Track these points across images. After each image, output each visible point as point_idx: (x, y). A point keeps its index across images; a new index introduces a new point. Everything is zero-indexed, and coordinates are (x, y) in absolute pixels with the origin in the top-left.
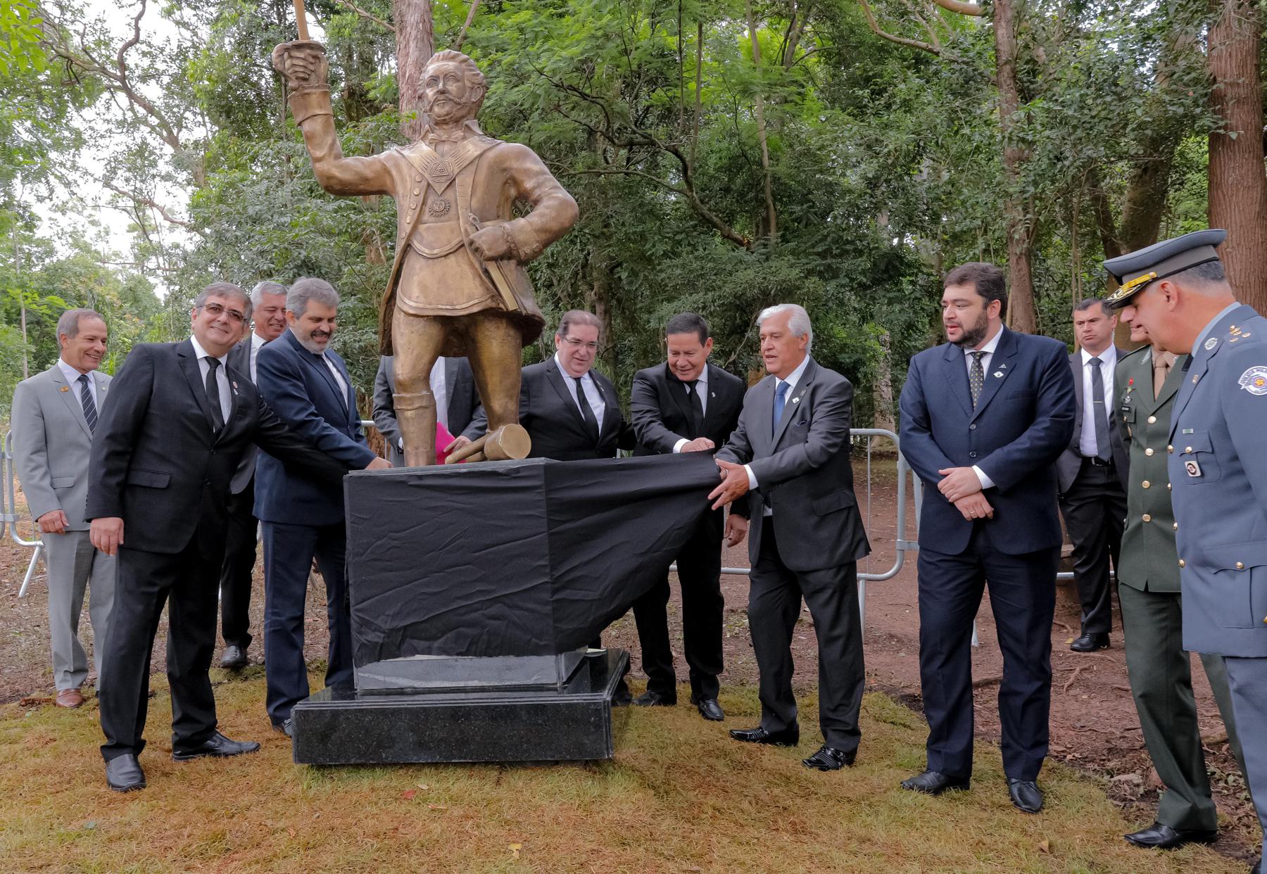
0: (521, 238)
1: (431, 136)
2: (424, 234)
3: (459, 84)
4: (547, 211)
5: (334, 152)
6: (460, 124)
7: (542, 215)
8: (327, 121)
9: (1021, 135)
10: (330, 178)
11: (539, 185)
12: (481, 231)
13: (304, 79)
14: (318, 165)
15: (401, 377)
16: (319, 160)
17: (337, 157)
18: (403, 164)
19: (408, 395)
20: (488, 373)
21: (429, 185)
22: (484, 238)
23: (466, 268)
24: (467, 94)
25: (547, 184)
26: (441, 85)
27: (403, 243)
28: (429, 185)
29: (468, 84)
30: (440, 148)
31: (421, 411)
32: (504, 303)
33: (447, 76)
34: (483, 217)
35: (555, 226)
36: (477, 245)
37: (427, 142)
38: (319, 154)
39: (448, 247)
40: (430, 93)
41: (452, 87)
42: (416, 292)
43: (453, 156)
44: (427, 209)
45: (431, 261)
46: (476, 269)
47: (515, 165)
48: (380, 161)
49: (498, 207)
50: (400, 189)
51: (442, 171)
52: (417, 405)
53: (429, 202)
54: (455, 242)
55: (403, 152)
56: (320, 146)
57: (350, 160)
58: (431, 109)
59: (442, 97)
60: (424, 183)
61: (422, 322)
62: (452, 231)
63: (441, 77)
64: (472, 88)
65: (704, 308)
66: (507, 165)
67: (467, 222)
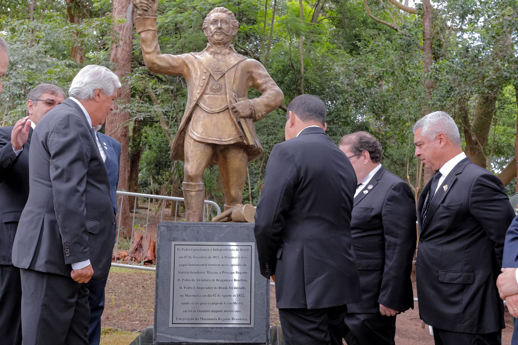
0: (258, 108)
1: (211, 50)
2: (207, 100)
3: (228, 25)
4: (270, 96)
5: (157, 50)
6: (226, 46)
7: (268, 98)
8: (155, 34)
9: (436, 76)
10: (153, 63)
11: (266, 82)
12: (238, 103)
13: (146, 11)
14: (147, 56)
15: (190, 174)
16: (148, 53)
17: (158, 53)
18: (196, 62)
19: (193, 184)
20: (231, 175)
21: (210, 75)
22: (240, 106)
23: (229, 120)
24: (231, 31)
25: (270, 82)
26: (219, 24)
27: (194, 103)
28: (210, 75)
29: (231, 26)
30: (216, 56)
31: (199, 192)
32: (247, 140)
33: (222, 21)
34: (239, 95)
35: (273, 104)
36: (237, 109)
37: (209, 52)
38: (149, 50)
39: (220, 108)
40: (212, 28)
41: (224, 26)
42: (200, 129)
43: (224, 62)
44: (209, 87)
45: (210, 115)
46: (234, 122)
47: (255, 70)
48: (182, 58)
49: (244, 90)
50: (193, 75)
51: (218, 69)
52: (197, 189)
53: (210, 84)
54: (224, 106)
55: (195, 56)
56: (150, 46)
57: (164, 55)
58: (212, 36)
59: (219, 31)
60: (208, 74)
61: (202, 146)
62: (222, 100)
63: (219, 20)
64: (233, 28)
65: (267, 143)
66: (250, 70)
67: (231, 96)
